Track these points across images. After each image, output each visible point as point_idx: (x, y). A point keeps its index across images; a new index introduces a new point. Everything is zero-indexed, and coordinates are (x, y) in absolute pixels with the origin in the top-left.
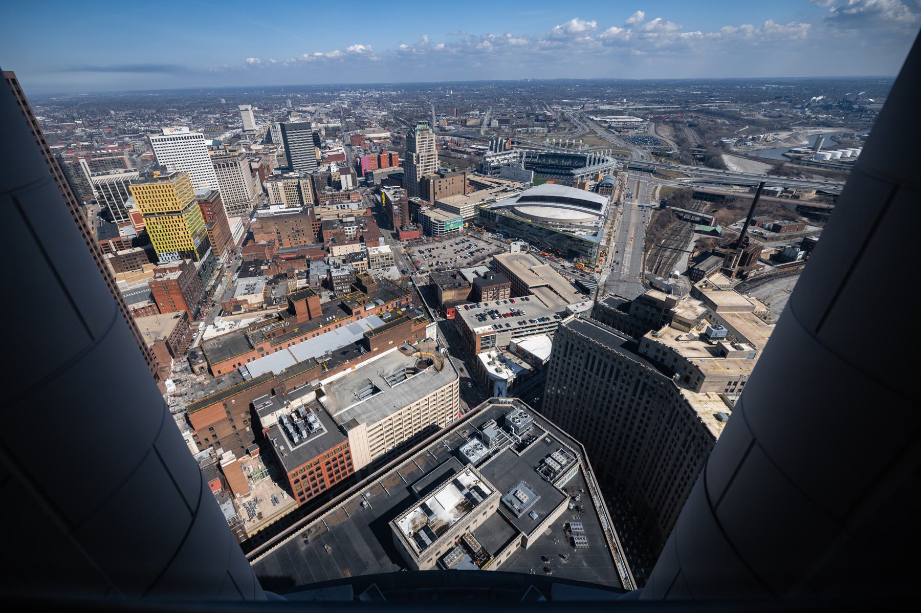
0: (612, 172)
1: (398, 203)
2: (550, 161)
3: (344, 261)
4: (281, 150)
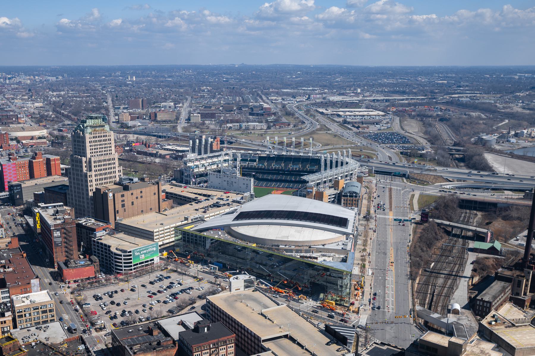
1: (62, 227)
2: (274, 166)
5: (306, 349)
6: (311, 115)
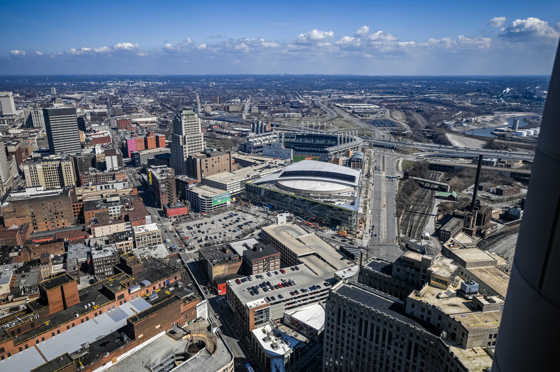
0: (360, 149)
1: (166, 181)
3: (107, 242)
4: (42, 133)
5: (327, 263)
6: (331, 108)
